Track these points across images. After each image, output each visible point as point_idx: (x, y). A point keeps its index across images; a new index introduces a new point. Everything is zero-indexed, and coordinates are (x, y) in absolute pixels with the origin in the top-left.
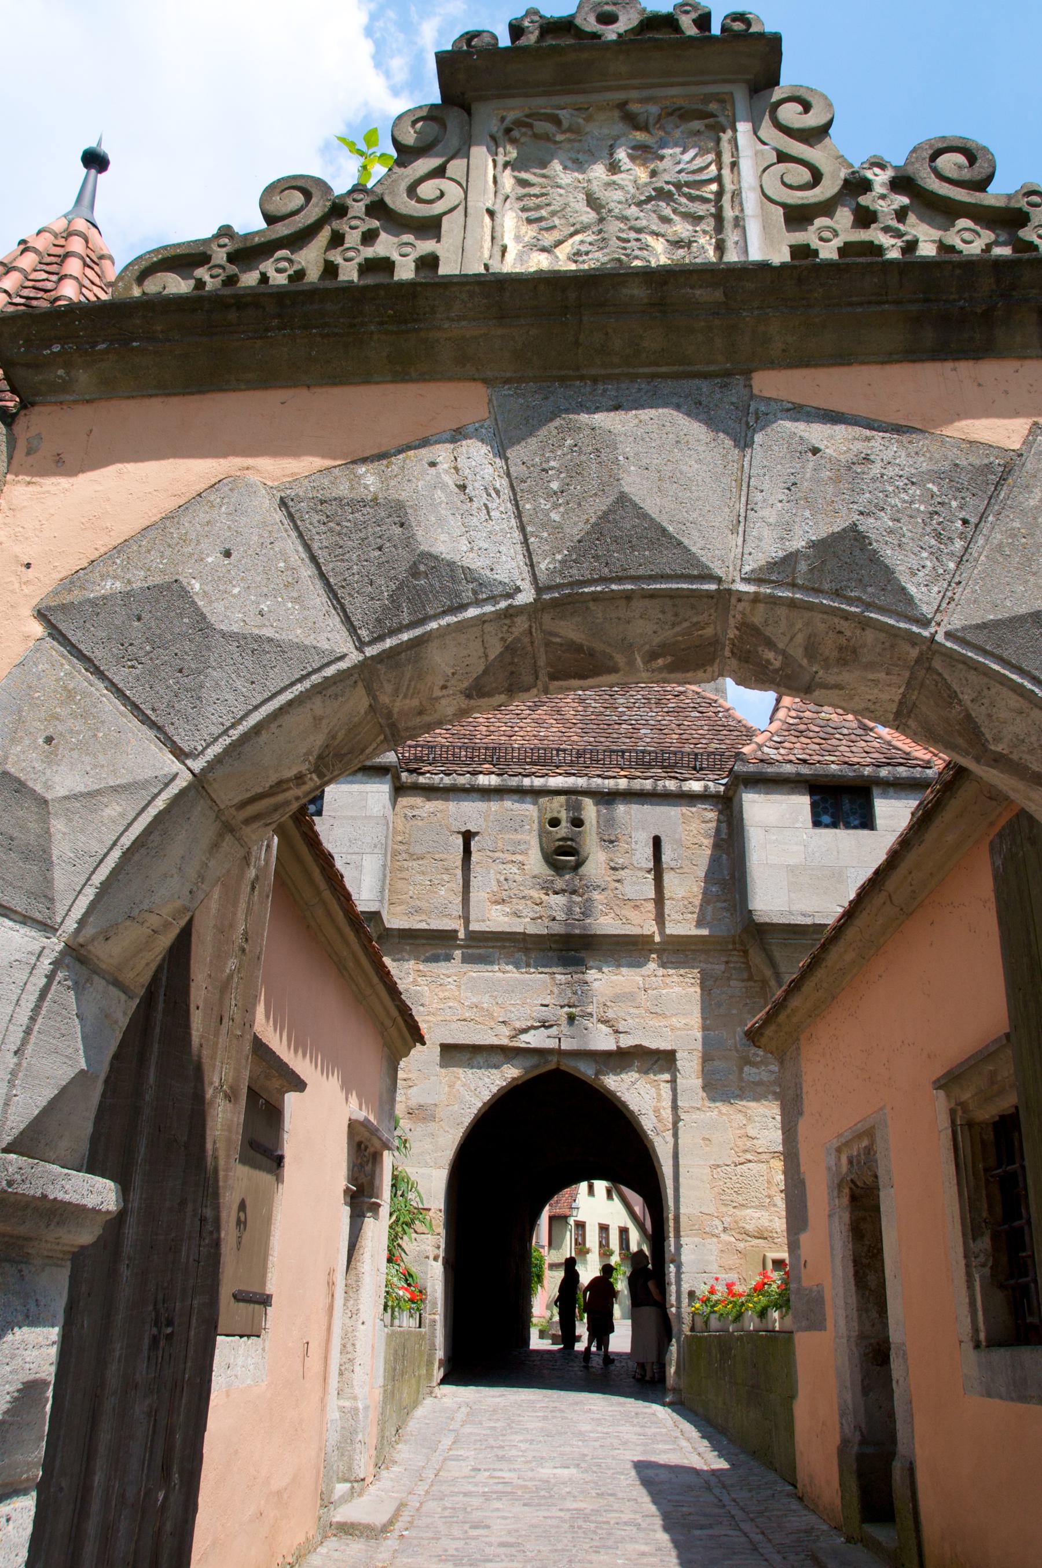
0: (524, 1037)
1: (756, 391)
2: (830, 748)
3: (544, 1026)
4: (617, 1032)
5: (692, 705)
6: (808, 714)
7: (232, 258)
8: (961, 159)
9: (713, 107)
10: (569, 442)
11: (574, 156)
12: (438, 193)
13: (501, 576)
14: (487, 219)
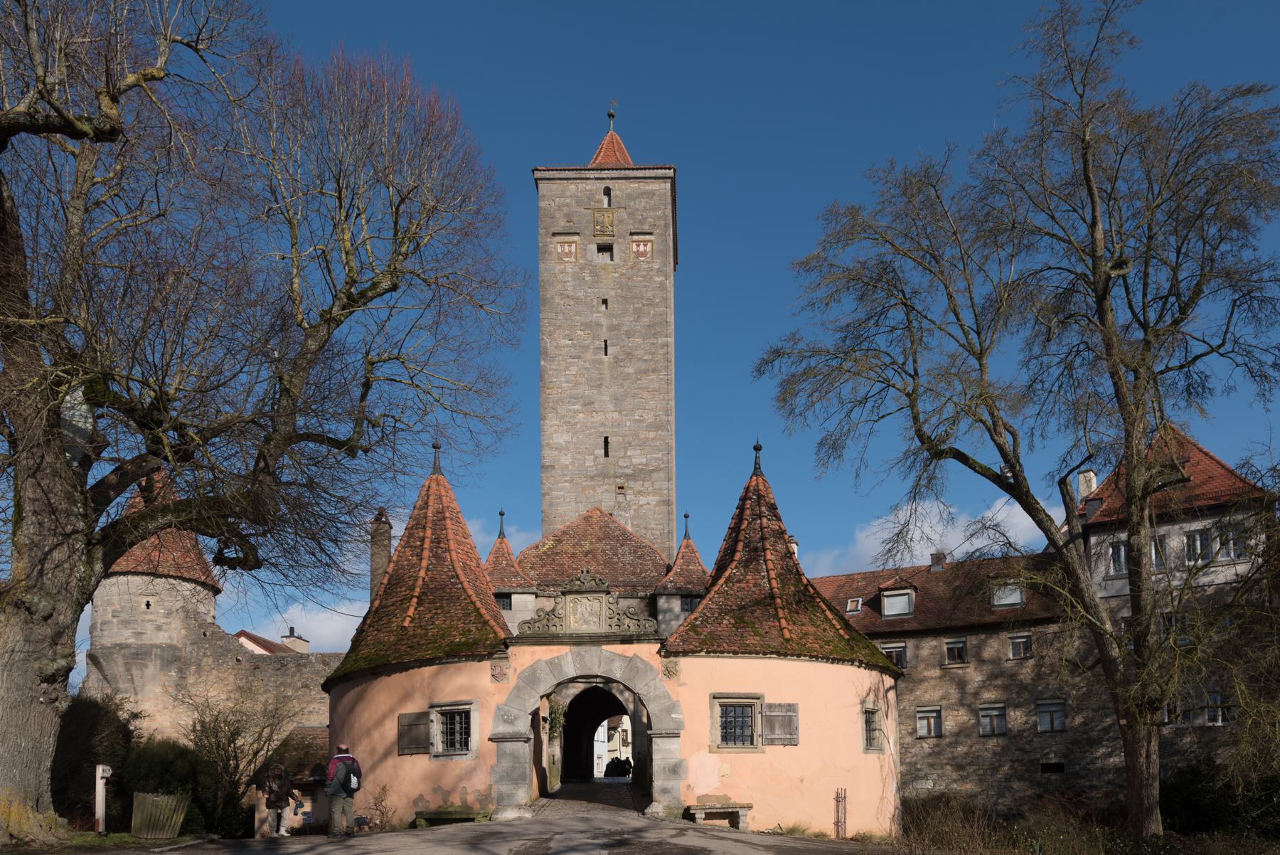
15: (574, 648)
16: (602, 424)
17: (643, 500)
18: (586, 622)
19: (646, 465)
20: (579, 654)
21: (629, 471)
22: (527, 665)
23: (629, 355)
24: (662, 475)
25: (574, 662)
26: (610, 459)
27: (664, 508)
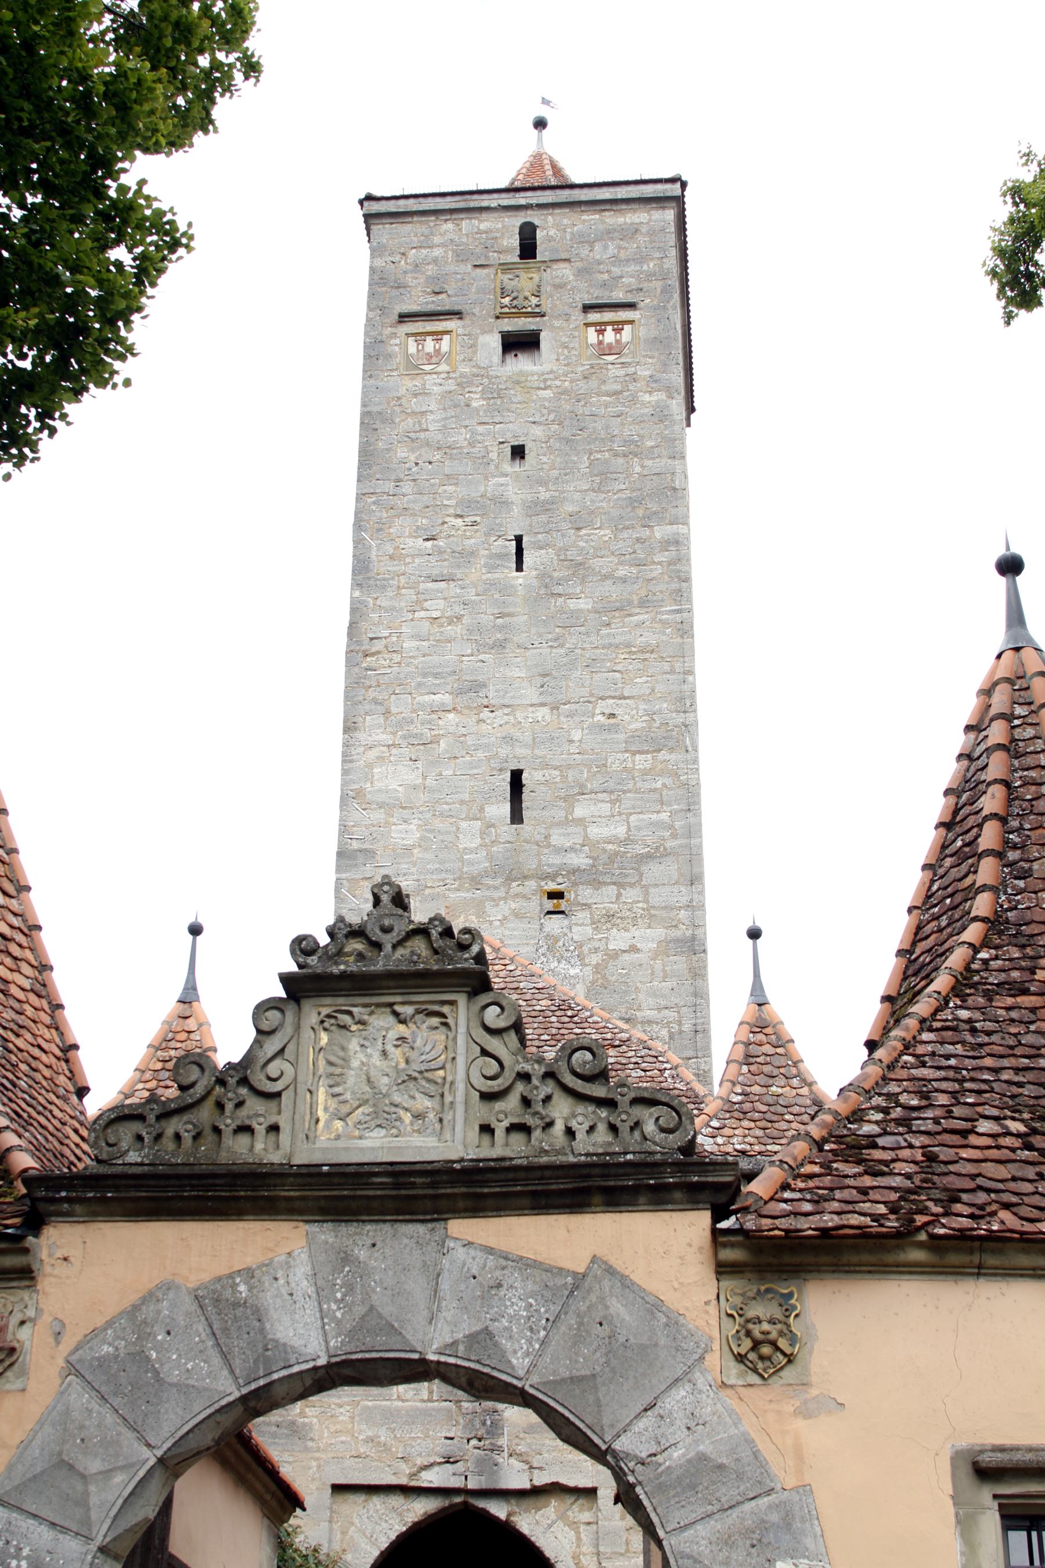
0: (424, 1475)
1: (449, 1233)
2: (775, 1133)
3: (448, 1462)
4: (531, 1467)
5: (633, 1060)
6: (756, 1089)
7: (159, 1118)
8: (588, 1056)
9: (446, 1009)
10: (347, 1269)
11: (362, 1042)
12: (279, 1073)
13: (309, 1350)
14: (308, 1095)
15: (326, 1234)
16: (509, 740)
17: (618, 940)
18: (384, 1115)
19: (628, 841)
20: (346, 1258)
21: (580, 860)
22: (114, 1304)
23: (579, 569)
24: (670, 869)
25: (321, 1294)
26: (526, 828)
27: (679, 963)
